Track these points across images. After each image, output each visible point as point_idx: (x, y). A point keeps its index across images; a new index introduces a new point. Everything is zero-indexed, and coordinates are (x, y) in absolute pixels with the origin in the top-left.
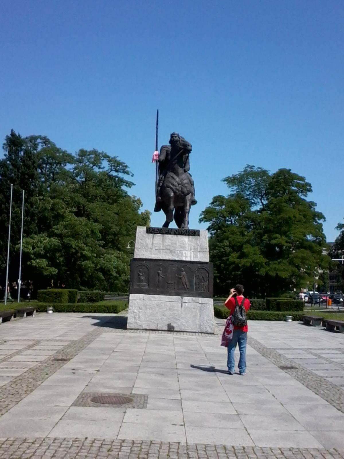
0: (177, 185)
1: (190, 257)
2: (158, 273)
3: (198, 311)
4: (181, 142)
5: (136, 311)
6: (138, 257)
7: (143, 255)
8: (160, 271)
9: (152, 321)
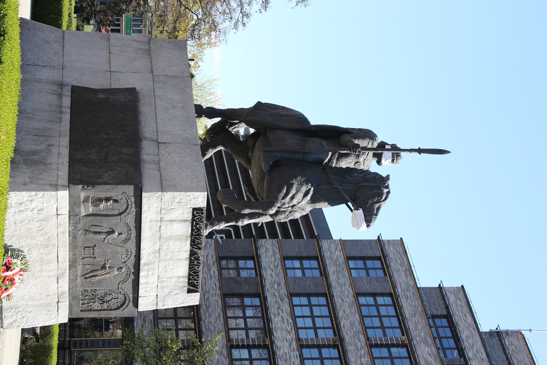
0: (291, 205)
1: (147, 283)
2: (113, 232)
4: (377, 205)
5: (34, 204)
6: (144, 201)
7: (149, 208)
8: (117, 234)
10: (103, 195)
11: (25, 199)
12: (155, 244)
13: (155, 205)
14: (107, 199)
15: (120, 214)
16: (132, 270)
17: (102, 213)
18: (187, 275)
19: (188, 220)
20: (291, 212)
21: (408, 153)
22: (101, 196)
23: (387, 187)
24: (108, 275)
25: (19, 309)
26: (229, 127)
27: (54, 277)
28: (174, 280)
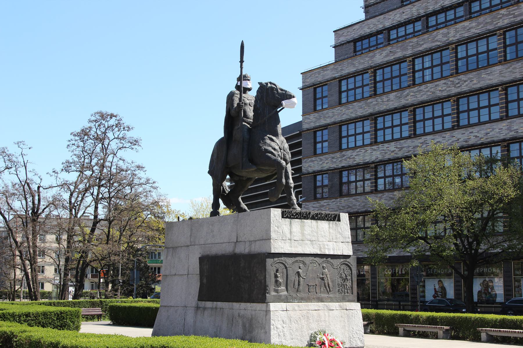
0: (279, 150)
1: (334, 250)
2: (298, 273)
3: (346, 321)
4: (279, 91)
5: (279, 326)
6: (277, 251)
7: (282, 248)
9: (299, 338)
10: (273, 280)
11: (276, 332)
12: (306, 244)
13: (280, 244)
14: (276, 276)
15: (286, 268)
16: (325, 259)
17: (285, 280)
18: (328, 222)
21: (243, 69)
22: (274, 281)
23: (267, 84)
24: (328, 276)
25: (351, 336)
27: (329, 313)
28: (331, 231)
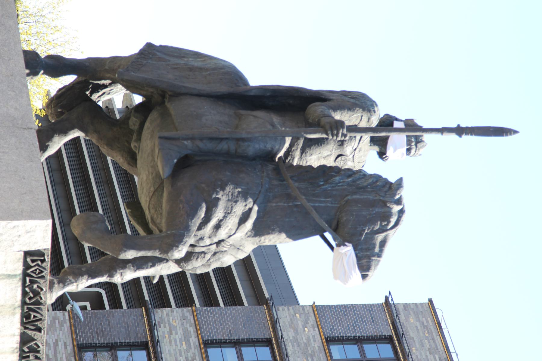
0: (216, 240)
4: (380, 237)
19: (15, 276)
20: (215, 254)
21: (438, 136)
23: (399, 202)
26: (92, 93)
